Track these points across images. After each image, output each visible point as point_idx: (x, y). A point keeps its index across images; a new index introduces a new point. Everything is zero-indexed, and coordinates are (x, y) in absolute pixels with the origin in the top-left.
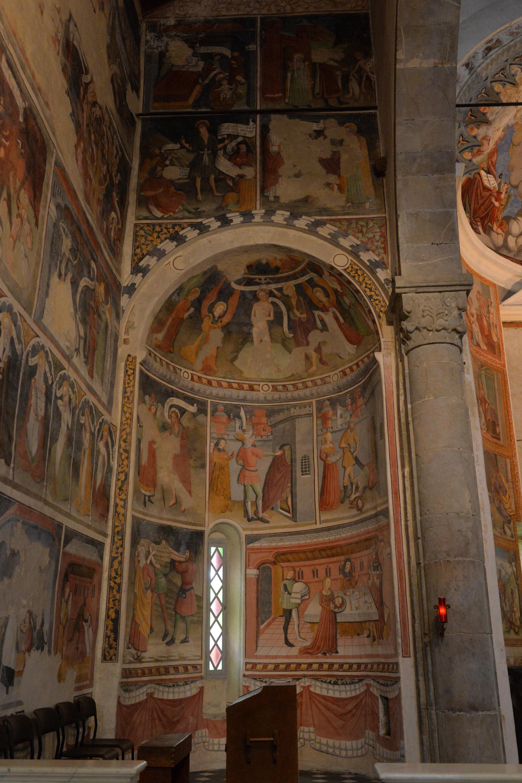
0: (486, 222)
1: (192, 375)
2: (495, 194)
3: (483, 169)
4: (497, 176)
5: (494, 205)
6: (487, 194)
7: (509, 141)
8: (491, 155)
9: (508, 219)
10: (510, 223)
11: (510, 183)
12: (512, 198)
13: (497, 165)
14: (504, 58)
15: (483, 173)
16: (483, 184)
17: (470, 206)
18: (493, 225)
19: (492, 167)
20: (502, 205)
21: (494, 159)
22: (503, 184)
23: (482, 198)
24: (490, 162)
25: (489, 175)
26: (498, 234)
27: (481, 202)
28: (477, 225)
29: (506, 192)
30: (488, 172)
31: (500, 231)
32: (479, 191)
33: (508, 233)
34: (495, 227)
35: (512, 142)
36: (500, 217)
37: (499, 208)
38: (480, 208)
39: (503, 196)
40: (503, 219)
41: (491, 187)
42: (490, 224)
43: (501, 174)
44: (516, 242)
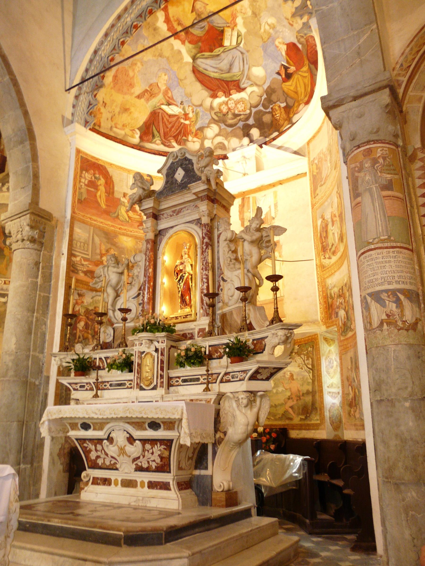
0: (180, 137)
1: (5, 281)
2: (183, 117)
3: (162, 104)
4: (179, 104)
5: (184, 124)
6: (174, 119)
7: (176, 79)
8: (166, 93)
9: (201, 129)
10: (205, 131)
11: (194, 105)
12: (201, 114)
13: (175, 98)
14: (115, 37)
15: (163, 107)
16: (167, 114)
17: (159, 132)
18: (188, 138)
19: (171, 101)
20: (192, 121)
21: (170, 95)
22: (187, 108)
23: (170, 123)
24: (167, 98)
25: (170, 106)
26: (194, 142)
27: (170, 126)
28: (170, 142)
29: (193, 112)
30: (169, 104)
31: (195, 139)
32: (165, 119)
33: (203, 139)
34: (190, 138)
35: (178, 79)
36: (194, 130)
37: (190, 125)
38: (170, 130)
39: (191, 115)
40: (196, 131)
41: (177, 113)
42: (184, 138)
43: (182, 102)
44: (212, 142)
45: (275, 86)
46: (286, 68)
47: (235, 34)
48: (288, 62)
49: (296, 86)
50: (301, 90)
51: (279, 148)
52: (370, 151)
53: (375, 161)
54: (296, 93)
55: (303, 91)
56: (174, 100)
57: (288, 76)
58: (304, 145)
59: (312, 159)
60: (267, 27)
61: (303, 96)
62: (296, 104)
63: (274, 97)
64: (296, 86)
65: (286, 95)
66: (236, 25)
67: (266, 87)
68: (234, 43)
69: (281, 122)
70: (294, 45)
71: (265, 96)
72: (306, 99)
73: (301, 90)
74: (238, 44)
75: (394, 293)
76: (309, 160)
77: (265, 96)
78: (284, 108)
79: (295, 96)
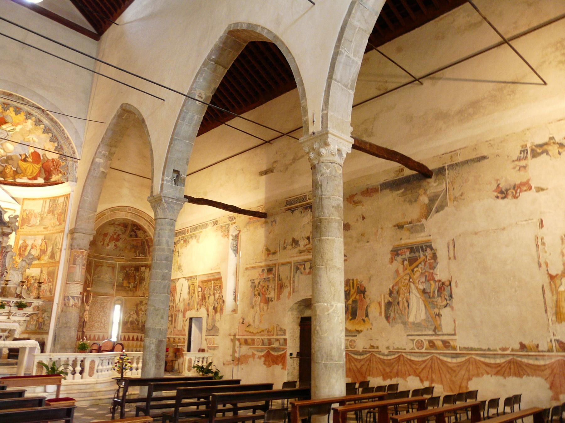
45: (14, 157)
46: (26, 157)
47: (12, 128)
48: (29, 155)
49: (27, 167)
50: (29, 171)
51: (4, 190)
52: (82, 252)
53: (83, 256)
54: (26, 170)
55: (30, 172)
56: (95, 270)
57: (25, 160)
58: (20, 199)
59: (24, 208)
60: (31, 139)
61: (28, 174)
62: (22, 174)
63: (10, 162)
64: (27, 167)
65: (18, 167)
66: (16, 126)
67: (9, 155)
68: (8, 129)
69: (8, 175)
70: (39, 155)
71: (5, 158)
72: (30, 177)
73: (29, 171)
74: (9, 131)
75: (77, 297)
76: (22, 207)
77: (5, 158)
78: (14, 171)
79: (24, 171)
